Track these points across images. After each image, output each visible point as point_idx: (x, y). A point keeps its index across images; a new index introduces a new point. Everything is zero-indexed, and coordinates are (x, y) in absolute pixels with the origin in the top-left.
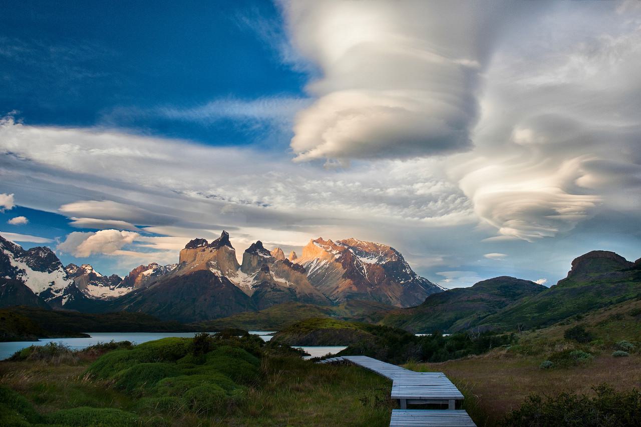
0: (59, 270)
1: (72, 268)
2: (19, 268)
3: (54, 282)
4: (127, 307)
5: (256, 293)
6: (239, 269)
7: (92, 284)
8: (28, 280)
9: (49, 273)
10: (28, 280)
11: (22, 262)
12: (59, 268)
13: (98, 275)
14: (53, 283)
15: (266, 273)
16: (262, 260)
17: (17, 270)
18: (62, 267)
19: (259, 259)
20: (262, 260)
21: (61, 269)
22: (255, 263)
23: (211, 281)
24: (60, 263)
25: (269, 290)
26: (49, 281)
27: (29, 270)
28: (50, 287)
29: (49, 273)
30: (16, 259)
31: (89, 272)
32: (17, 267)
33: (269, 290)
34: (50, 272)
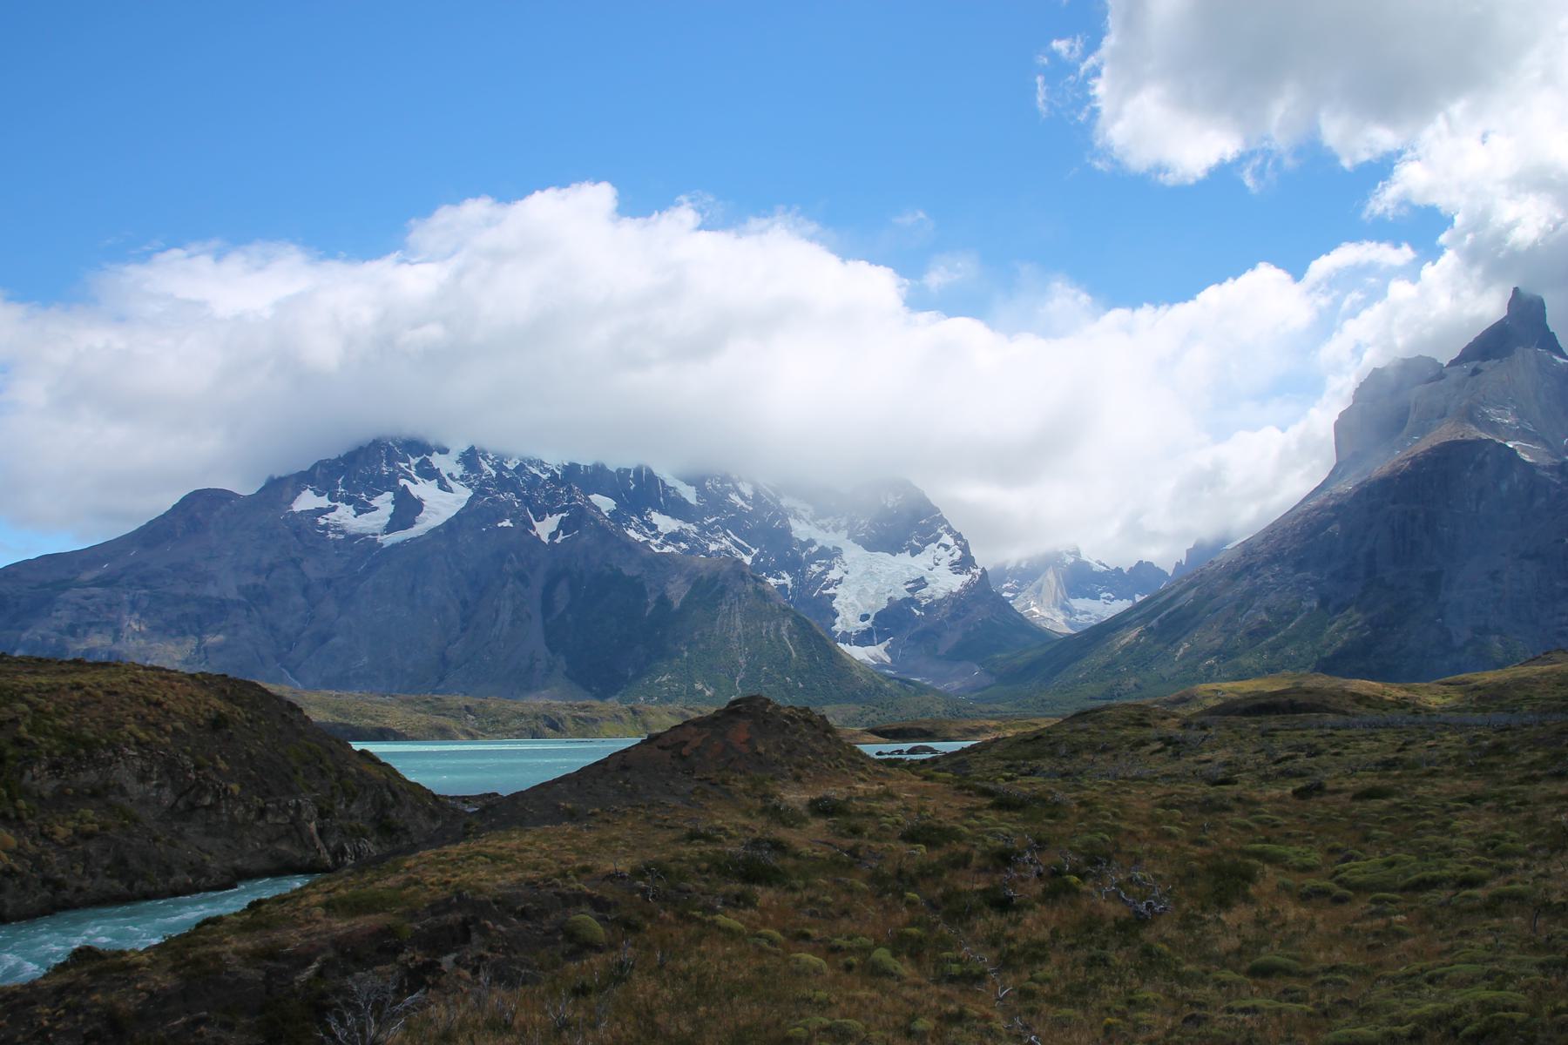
2: (820, 543)
4: (1134, 633)
8: (846, 577)
9: (913, 555)
10: (846, 577)
11: (836, 529)
12: (940, 536)
14: (920, 583)
17: (814, 549)
18: (949, 530)
21: (947, 539)
24: (942, 521)
26: (907, 576)
27: (854, 554)
28: (909, 595)
29: (913, 555)
30: (821, 522)
32: (811, 542)
34: (915, 551)
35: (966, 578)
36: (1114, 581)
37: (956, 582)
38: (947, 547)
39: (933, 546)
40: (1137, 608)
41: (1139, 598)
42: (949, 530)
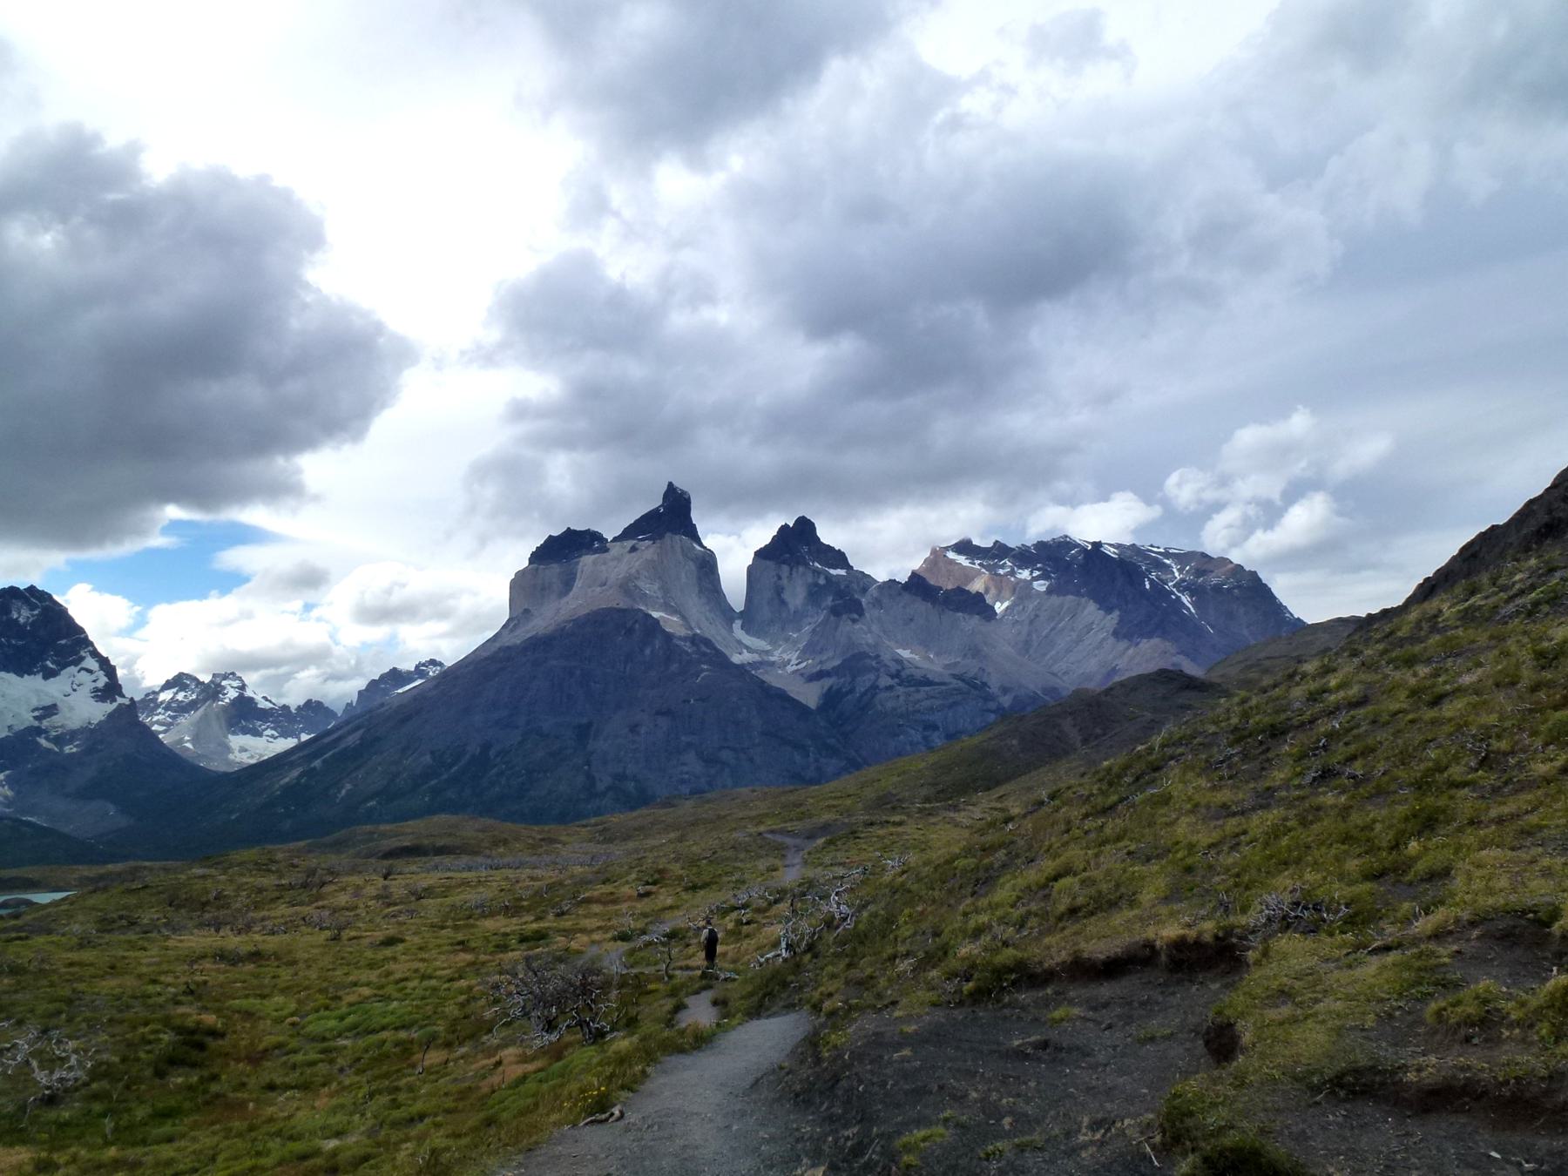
0: (84, 664)
1: (184, 687)
3: (54, 706)
5: (831, 699)
6: (737, 624)
7: (245, 731)
12: (83, 659)
13: (263, 705)
14: (50, 710)
15: (854, 621)
16: (822, 581)
19: (810, 580)
20: (822, 581)
21: (91, 663)
22: (796, 596)
23: (648, 652)
25: (885, 681)
26: (35, 703)
28: (36, 723)
31: (232, 694)
33: (885, 681)
34: (49, 674)
35: (109, 707)
36: (282, 719)
37: (98, 712)
38: (90, 671)
39: (72, 669)
40: (301, 747)
41: (305, 737)
42: (95, 654)
